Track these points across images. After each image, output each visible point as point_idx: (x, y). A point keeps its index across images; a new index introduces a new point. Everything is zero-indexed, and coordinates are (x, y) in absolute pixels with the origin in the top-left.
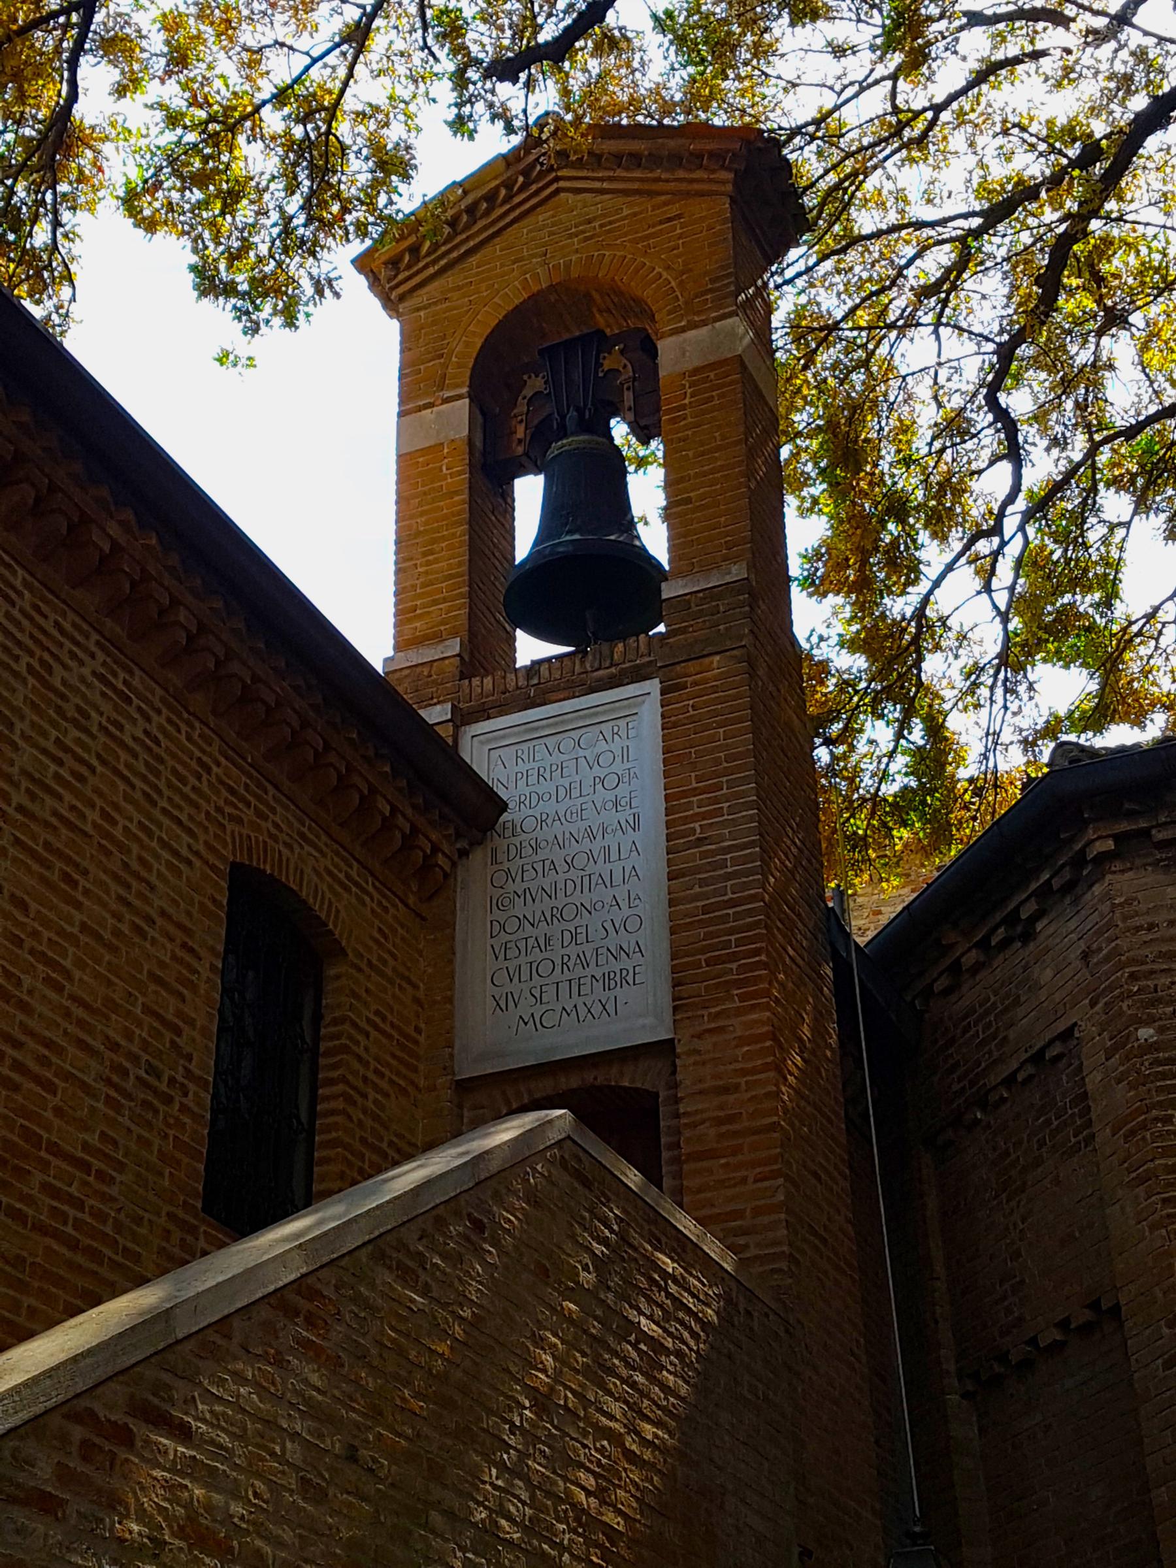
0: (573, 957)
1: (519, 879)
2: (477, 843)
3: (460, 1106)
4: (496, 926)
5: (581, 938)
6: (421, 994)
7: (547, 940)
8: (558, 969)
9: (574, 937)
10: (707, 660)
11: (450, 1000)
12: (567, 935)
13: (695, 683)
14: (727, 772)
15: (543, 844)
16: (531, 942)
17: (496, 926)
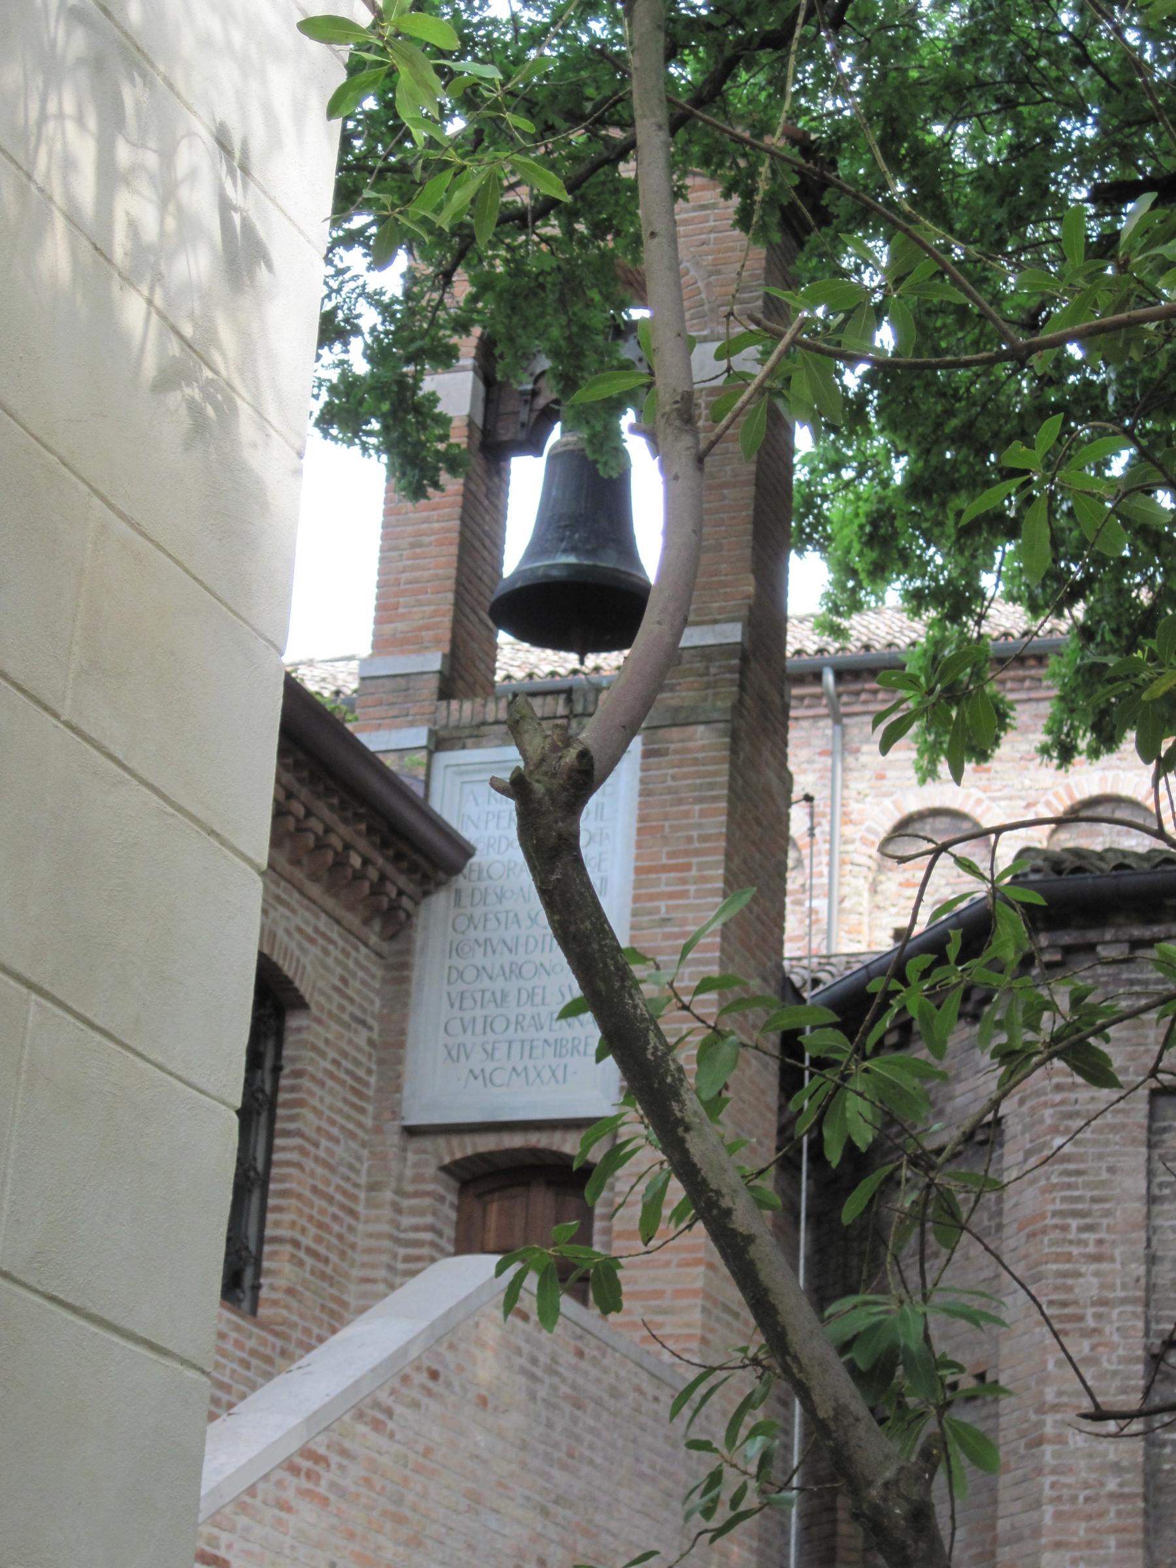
0: (528, 1018)
1: (480, 926)
2: (439, 884)
3: (404, 1150)
4: (454, 974)
5: (538, 999)
6: (375, 1036)
7: (504, 995)
8: (512, 1027)
9: (531, 996)
10: (691, 729)
11: (401, 1045)
12: (524, 996)
13: (676, 752)
14: (697, 853)
15: (508, 894)
16: (488, 995)
17: (454, 974)
